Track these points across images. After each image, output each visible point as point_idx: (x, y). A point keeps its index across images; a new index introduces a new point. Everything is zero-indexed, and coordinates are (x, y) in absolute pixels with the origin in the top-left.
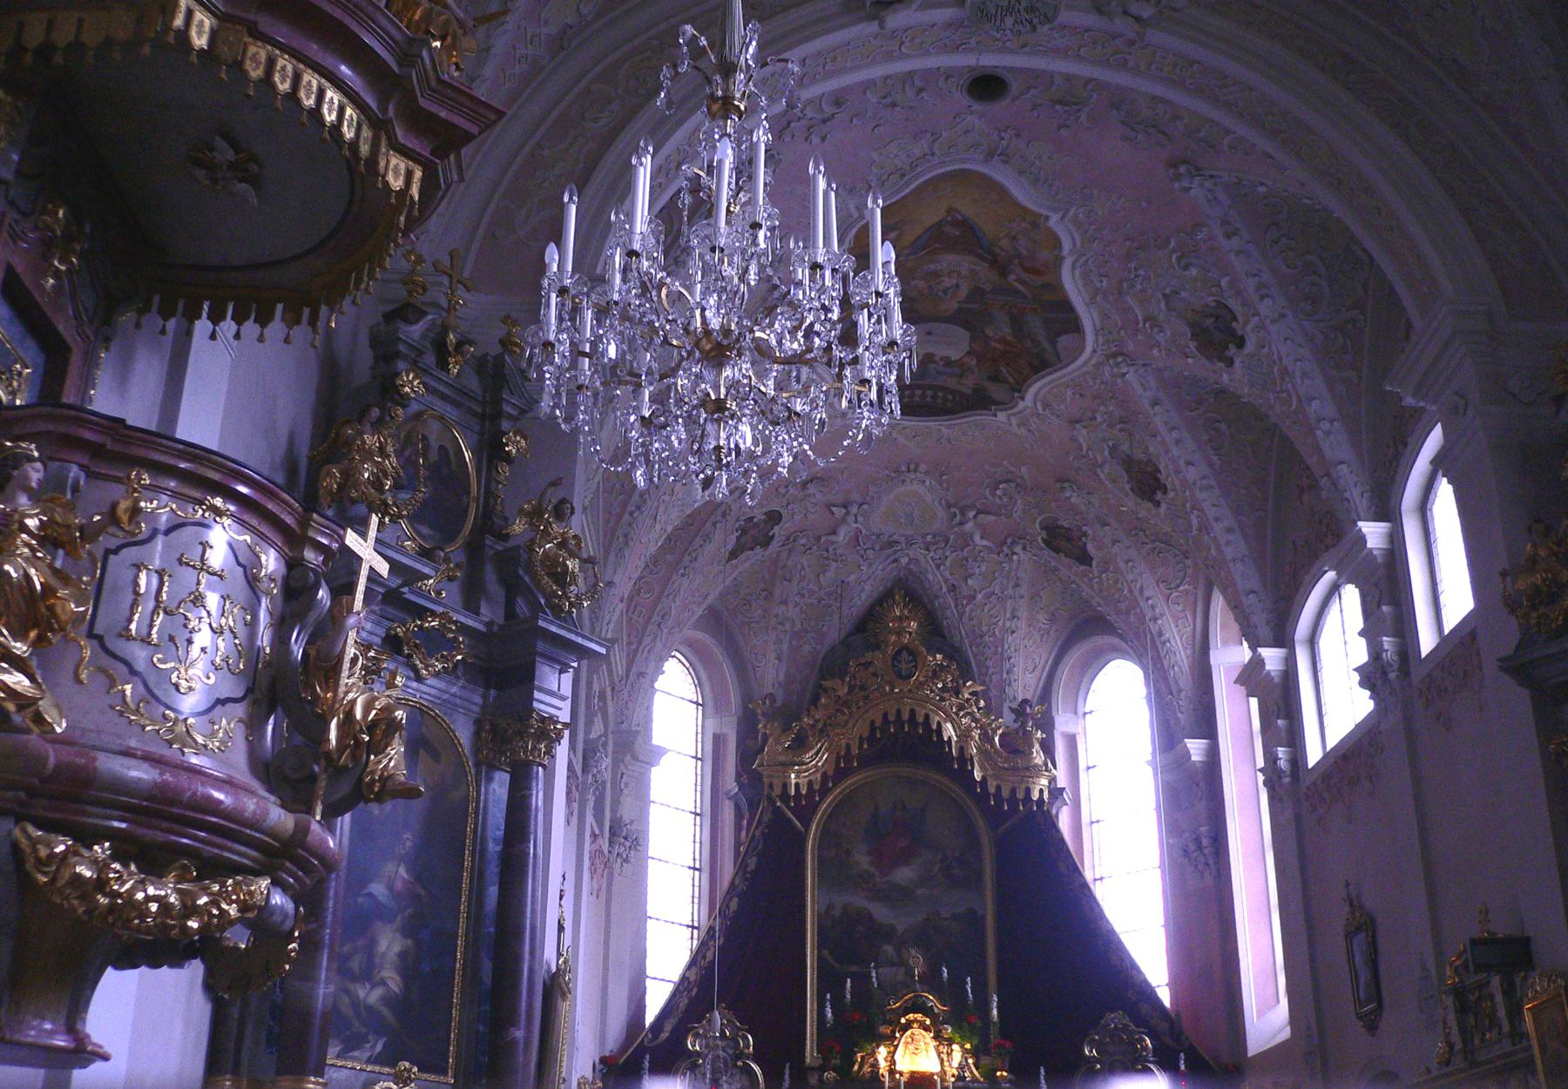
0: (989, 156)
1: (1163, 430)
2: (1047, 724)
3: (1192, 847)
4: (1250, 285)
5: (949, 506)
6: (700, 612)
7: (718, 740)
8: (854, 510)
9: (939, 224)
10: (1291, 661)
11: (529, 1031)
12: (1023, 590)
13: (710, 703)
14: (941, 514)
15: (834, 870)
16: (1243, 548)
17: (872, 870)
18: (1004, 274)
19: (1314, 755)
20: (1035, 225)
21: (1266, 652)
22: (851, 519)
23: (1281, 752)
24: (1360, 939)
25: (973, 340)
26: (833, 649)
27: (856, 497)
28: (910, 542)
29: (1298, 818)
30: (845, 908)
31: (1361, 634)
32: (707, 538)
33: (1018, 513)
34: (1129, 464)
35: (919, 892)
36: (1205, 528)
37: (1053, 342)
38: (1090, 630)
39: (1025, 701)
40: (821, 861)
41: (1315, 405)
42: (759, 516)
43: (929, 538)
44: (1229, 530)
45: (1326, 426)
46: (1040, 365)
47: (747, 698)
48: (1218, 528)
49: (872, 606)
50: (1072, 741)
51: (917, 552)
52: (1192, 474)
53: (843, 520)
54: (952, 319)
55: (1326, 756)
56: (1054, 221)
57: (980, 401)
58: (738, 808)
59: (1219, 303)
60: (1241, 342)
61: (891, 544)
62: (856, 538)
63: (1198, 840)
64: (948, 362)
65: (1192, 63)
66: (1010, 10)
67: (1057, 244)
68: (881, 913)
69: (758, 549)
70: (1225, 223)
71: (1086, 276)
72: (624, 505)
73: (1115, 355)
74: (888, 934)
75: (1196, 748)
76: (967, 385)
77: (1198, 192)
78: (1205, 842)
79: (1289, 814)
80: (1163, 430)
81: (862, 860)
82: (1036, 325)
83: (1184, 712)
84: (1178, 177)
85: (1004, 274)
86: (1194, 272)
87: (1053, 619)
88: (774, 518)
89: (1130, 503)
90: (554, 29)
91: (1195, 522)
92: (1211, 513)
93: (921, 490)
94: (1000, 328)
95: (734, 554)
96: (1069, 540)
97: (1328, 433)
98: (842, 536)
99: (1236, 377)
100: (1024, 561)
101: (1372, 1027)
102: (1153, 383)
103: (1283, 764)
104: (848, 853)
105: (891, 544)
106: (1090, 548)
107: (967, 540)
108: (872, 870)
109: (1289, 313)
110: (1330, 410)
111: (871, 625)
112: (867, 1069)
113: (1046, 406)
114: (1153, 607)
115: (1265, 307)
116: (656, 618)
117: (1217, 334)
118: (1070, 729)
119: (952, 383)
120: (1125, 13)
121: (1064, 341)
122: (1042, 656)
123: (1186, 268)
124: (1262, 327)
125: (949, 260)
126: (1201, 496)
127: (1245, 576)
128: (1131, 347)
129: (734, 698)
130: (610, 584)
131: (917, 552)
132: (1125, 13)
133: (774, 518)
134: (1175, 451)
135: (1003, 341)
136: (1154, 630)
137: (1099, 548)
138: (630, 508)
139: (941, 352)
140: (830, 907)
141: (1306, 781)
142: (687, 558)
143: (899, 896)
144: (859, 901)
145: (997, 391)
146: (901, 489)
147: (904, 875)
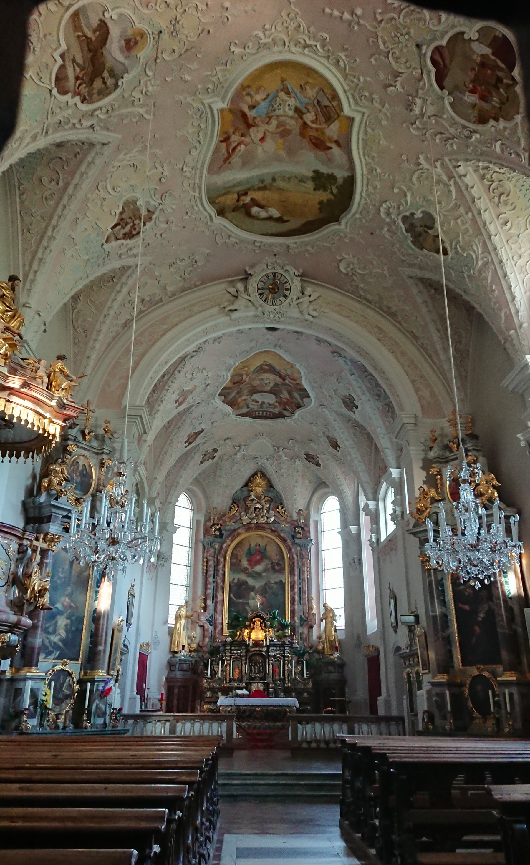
0: (275, 346)
1: (337, 428)
2: (307, 518)
3: (352, 562)
4: (358, 390)
5: (274, 446)
6: (191, 481)
7: (198, 522)
8: (242, 447)
9: (261, 365)
10: (377, 505)
11: (105, 647)
12: (300, 473)
13: (195, 511)
14: (271, 448)
15: (235, 566)
16: (364, 468)
17: (248, 567)
18: (284, 379)
19: (383, 537)
20: (292, 367)
21: (369, 502)
22: (241, 450)
23: (373, 536)
24: (392, 601)
25: (276, 398)
26: (236, 492)
27: (243, 443)
28: (261, 458)
29: (379, 558)
30: (238, 580)
31: (392, 503)
32: (193, 458)
33: (296, 449)
34: (328, 437)
35: (264, 574)
36: (352, 461)
37: (302, 400)
38: (322, 486)
39: (300, 510)
40: (231, 564)
41: (379, 429)
42: (210, 450)
43: (268, 456)
44: (359, 462)
45: (382, 436)
46: (299, 406)
47: (208, 508)
48: (356, 461)
49: (250, 478)
50: (316, 523)
51: (264, 460)
52: (347, 443)
53: (239, 451)
54: (271, 392)
55: (387, 537)
56: (298, 366)
57: (280, 416)
58: (203, 545)
59: (350, 395)
60: (357, 407)
61: (255, 458)
62: (244, 455)
63: (354, 559)
64: (270, 404)
65: (331, 329)
66: (272, 313)
67: (299, 372)
68: (251, 581)
69: (210, 460)
70: (350, 370)
71: (310, 382)
72: (160, 453)
73: (321, 405)
74: (253, 589)
75: (353, 529)
76: (276, 411)
77: (341, 361)
78: (356, 561)
79: (376, 556)
80: (337, 428)
81: (245, 563)
82: (296, 395)
83: (349, 517)
84: (334, 356)
85: (284, 379)
86: (341, 384)
87: (310, 482)
88: (215, 450)
89: (331, 449)
90: (123, 321)
91: (349, 458)
92: (354, 456)
93: (264, 441)
94: (285, 395)
95: (202, 462)
96: (313, 459)
97: (383, 438)
98: (239, 456)
99: (356, 416)
100: (300, 464)
101: (396, 632)
102: (334, 414)
103: (374, 540)
104: (240, 561)
105: (255, 458)
106: (320, 462)
107: (280, 457)
108: (248, 567)
109: (371, 399)
110: (384, 431)
111: (250, 484)
112: (241, 637)
113: (302, 418)
114: (340, 481)
115: (363, 397)
116: (175, 484)
117: (350, 403)
118: (316, 519)
119: (271, 410)
120: (309, 314)
121: (305, 400)
122: (307, 495)
123: (339, 383)
124: (363, 404)
125: (266, 376)
126: (350, 450)
127: (365, 477)
128: (326, 403)
129: (204, 506)
130: (156, 478)
131: (264, 460)
132: (309, 314)
133: (215, 450)
134: (342, 436)
135: (286, 399)
136: (341, 488)
137: (323, 462)
138: (163, 453)
139: (266, 401)
140: (234, 579)
141: (381, 546)
142: (185, 465)
143: (257, 576)
144: (243, 577)
145: (286, 413)
146: (258, 441)
147: (258, 568)
